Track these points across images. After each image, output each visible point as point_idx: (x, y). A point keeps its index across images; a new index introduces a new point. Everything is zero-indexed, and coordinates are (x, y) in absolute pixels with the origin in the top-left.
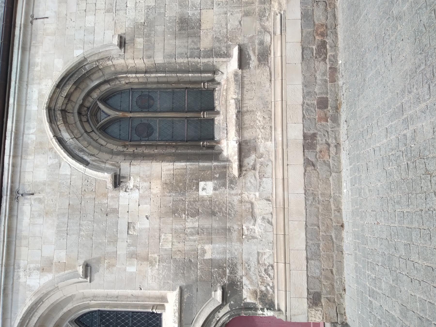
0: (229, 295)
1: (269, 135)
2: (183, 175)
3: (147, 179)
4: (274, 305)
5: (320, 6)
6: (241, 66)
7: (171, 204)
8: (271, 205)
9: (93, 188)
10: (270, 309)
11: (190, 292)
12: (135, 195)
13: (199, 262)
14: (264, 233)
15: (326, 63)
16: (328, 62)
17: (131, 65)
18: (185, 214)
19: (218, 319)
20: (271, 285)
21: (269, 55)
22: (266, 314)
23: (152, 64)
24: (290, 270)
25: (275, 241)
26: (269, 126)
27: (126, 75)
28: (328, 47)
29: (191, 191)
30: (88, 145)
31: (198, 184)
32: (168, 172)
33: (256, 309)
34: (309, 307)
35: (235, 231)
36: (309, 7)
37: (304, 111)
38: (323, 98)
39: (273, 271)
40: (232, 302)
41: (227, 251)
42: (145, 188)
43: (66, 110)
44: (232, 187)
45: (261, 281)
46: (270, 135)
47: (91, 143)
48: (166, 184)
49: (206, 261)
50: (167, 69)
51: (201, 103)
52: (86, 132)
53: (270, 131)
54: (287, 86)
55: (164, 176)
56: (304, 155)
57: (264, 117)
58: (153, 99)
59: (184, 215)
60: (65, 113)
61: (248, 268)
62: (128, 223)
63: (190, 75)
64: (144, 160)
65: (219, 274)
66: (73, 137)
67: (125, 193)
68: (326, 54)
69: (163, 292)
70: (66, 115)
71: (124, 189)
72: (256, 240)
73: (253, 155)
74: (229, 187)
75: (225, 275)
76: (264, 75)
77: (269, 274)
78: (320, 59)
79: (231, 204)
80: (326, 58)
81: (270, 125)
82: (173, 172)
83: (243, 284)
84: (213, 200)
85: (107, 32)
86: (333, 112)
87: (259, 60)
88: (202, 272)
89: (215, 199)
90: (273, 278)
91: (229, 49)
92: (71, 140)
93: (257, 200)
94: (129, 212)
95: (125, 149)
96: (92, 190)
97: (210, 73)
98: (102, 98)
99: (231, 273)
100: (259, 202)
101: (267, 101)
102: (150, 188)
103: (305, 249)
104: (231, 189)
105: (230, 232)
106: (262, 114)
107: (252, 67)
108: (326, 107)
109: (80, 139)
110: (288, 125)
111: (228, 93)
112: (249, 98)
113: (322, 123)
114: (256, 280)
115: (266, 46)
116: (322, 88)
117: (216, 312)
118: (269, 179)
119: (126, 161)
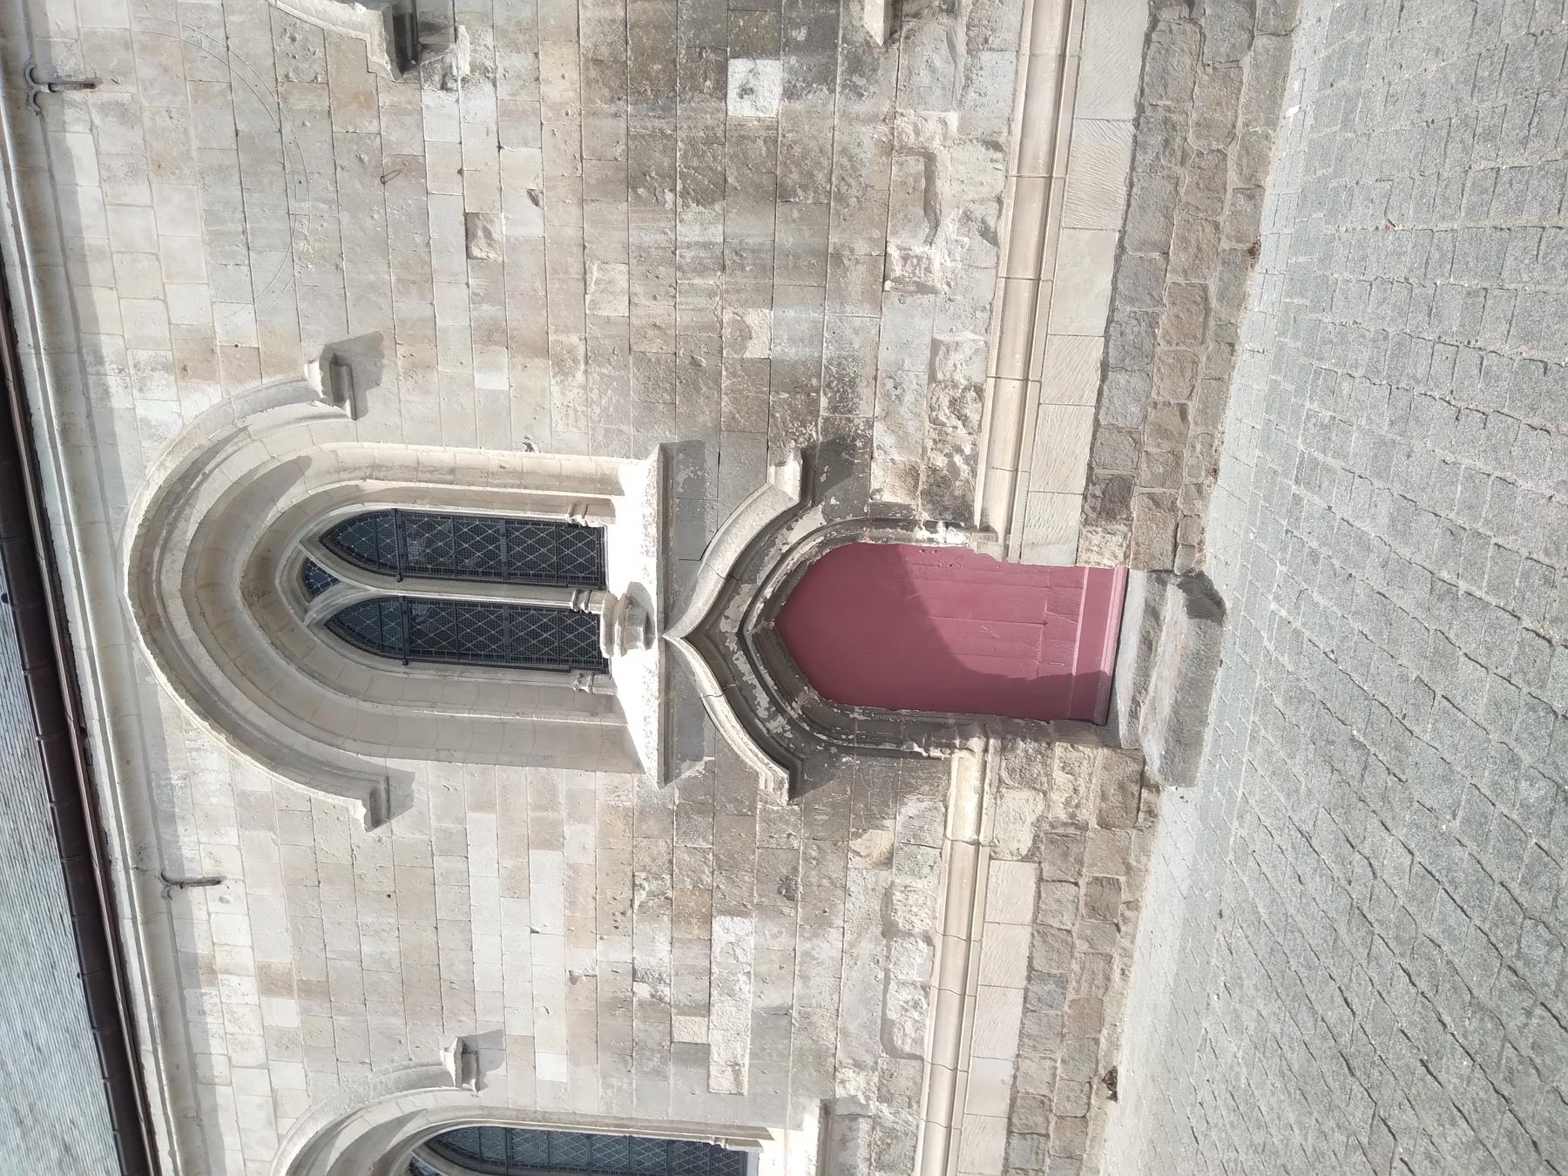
4: (971, 514)
7: (620, 149)
8: (999, 166)
10: (957, 526)
12: (482, 103)
20: (967, 450)
22: (941, 540)
31: (723, 69)
33: (910, 524)
35: (857, 262)
42: (518, 77)
45: (936, 437)
48: (598, 62)
61: (894, 392)
67: (442, 94)
71: (437, 78)
74: (844, 86)
77: (966, 416)
83: (875, 445)
84: (780, 139)
89: (790, 135)
93: (949, 143)
96: (316, 77)
102: (537, 79)
104: (851, 95)
105: (839, 267)
114: (919, 435)
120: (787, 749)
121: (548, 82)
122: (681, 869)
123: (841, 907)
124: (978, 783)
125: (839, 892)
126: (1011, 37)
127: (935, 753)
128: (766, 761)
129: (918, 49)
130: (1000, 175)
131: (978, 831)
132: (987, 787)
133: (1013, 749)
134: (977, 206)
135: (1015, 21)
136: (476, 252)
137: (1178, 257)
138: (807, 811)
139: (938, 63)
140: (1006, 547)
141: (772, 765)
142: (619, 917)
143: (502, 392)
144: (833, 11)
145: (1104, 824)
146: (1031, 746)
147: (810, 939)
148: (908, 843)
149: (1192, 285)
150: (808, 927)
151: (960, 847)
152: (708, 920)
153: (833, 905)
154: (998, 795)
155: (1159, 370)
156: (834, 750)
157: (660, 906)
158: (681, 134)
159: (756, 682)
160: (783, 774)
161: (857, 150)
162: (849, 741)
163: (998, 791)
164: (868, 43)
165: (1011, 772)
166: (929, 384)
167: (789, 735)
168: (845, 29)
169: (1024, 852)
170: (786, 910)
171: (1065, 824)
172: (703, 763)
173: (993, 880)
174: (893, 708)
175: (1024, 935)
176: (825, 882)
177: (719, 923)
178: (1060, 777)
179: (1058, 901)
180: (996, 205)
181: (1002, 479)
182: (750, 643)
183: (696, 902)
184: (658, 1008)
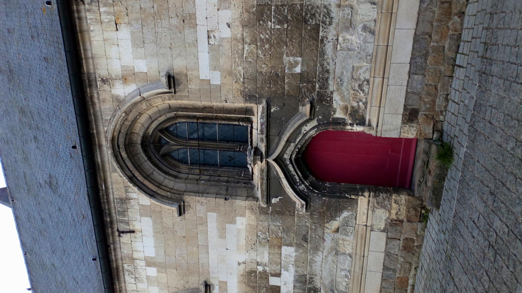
0: (317, 110)
4: (365, 121)
11: (276, 106)
13: (287, 76)
14: (363, 44)
18: (271, 21)
19: (305, 132)
20: (364, 100)
22: (355, 129)
24: (388, 85)
25: (374, 53)
33: (345, 124)
34: (403, 123)
35: (329, 42)
39: (368, 86)
40: (320, 117)
41: (318, 65)
45: (354, 96)
49: (293, 75)
59: (269, 23)
61: (340, 83)
62: (208, 31)
65: (308, 89)
69: (248, 105)
72: (353, 52)
75: (314, 90)
79: (327, 9)
84: (304, 4)
88: (289, 86)
89: (308, 3)
90: (367, 93)
93: (359, 3)
94: (208, 18)
99: (320, 88)
100: (361, 6)
103: (409, 62)
114: (348, 96)
117: (303, 126)
120: (305, 195)
122: (272, 231)
123: (322, 245)
124: (367, 207)
125: (322, 240)
127: (353, 197)
128: (298, 198)
130: (376, 13)
131: (367, 223)
132: (370, 208)
133: (379, 196)
134: (368, 23)
136: (211, 42)
137: (435, 37)
138: (311, 215)
140: (377, 132)
141: (300, 200)
142: (253, 245)
143: (218, 85)
145: (409, 221)
146: (385, 195)
147: (312, 254)
148: (344, 225)
149: (439, 46)
150: (312, 250)
151: (361, 227)
152: (280, 247)
153: (320, 244)
154: (373, 211)
155: (428, 74)
156: (320, 195)
157: (265, 242)
158: (273, 4)
159: (295, 174)
160: (304, 203)
161: (329, 7)
162: (325, 193)
163: (373, 209)
165: (378, 203)
166: (351, 80)
167: (306, 190)
169: (382, 229)
170: (305, 245)
171: (396, 220)
172: (278, 199)
173: (372, 237)
174: (339, 182)
175: (382, 255)
176: (317, 237)
177: (284, 248)
178: (394, 205)
179: (394, 245)
180: (374, 22)
181: (375, 110)
182: (293, 162)
183: (277, 241)
184: (265, 276)
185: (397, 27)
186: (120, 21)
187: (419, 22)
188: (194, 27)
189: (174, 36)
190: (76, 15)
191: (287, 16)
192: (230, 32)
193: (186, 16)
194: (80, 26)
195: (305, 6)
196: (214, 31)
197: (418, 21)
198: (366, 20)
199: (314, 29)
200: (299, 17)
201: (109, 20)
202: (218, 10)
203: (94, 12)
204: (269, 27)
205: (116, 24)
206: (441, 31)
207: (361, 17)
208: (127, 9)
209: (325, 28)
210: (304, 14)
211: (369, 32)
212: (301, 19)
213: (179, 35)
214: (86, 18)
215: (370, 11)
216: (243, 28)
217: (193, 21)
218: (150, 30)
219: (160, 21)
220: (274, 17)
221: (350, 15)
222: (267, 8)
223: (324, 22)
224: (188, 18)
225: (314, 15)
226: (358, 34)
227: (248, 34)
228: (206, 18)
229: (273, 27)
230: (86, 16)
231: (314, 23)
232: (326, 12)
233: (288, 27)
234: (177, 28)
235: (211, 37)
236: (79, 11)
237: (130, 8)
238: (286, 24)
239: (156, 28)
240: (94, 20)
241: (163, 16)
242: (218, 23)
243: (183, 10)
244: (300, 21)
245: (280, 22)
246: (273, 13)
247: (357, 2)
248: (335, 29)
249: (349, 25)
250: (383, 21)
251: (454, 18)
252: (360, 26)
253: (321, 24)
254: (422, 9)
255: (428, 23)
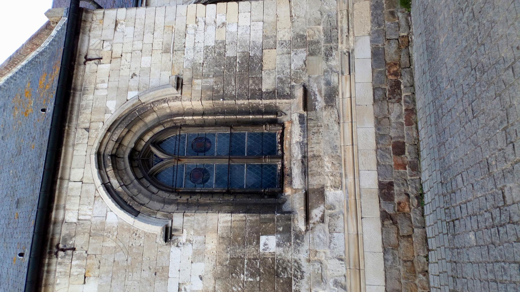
1: (339, 183)
2: (242, 229)
3: (201, 232)
5: (392, 44)
6: (305, 108)
7: (228, 262)
8: (343, 266)
9: (141, 242)
12: (188, 250)
15: (401, 105)
16: (403, 104)
17: (187, 107)
18: (243, 274)
21: (336, 96)
23: (210, 106)
26: (338, 173)
27: (182, 117)
28: (402, 87)
29: (251, 247)
30: (137, 193)
31: (258, 239)
32: (226, 225)
36: (380, 45)
37: (378, 157)
38: (399, 142)
42: (199, 243)
43: (117, 155)
44: (297, 243)
46: (340, 183)
47: (141, 190)
48: (223, 238)
50: (226, 111)
51: (262, 146)
52: (137, 178)
53: (340, 179)
54: (358, 130)
55: (221, 229)
56: (380, 206)
57: (332, 163)
58: (210, 142)
59: (242, 276)
60: (115, 159)
62: (179, 284)
63: (251, 117)
64: (198, 210)
66: (122, 184)
67: (177, 248)
68: (400, 95)
70: (116, 160)
71: (176, 244)
73: (321, 206)
74: (294, 243)
76: (331, 117)
78: (393, 100)
79: (298, 263)
80: (401, 99)
81: (340, 171)
82: (230, 225)
84: (276, 258)
85: (163, 73)
86: (412, 159)
87: (327, 102)
89: (279, 257)
91: (293, 90)
92: (120, 188)
94: (181, 271)
95: (178, 197)
97: (273, 115)
98: (155, 142)
100: (329, 261)
101: (336, 146)
102: (205, 243)
104: (296, 245)
106: (331, 160)
107: (318, 109)
108: (403, 152)
109: (129, 186)
110: (361, 172)
111: (293, 136)
112: (316, 141)
113: (400, 170)
115: (334, 87)
116: (398, 132)
118: (341, 234)
119: (179, 211)
121: (208, 243)
126: (342, 229)
129: (315, 232)
130: (344, 268)
134: (338, 278)
135: (342, 225)
139: (321, 236)
144: (290, 223)
161: (299, 261)
164: (300, 231)
168: (293, 227)
180: (344, 278)
185: (367, 283)
186: (90, 274)
187: (387, 279)
188: (165, 280)
189: (143, 289)
190: (46, 268)
191: (259, 269)
192: (202, 285)
193: (159, 269)
194: (47, 280)
195: (277, 260)
196: (185, 284)
197: (386, 278)
198: (336, 275)
199: (286, 282)
200: (271, 270)
201: (78, 273)
202: (192, 263)
203: (65, 265)
204: (242, 279)
205: (85, 277)
206: (411, 289)
207: (331, 272)
208: (100, 262)
209: (297, 282)
210: (276, 268)
211: (341, 287)
212: (273, 272)
213: (149, 288)
214: (55, 271)
215: (339, 267)
216: (215, 281)
217: (165, 274)
218: (119, 283)
219: (131, 274)
220: (247, 270)
221: (320, 270)
222: (239, 261)
223: (295, 276)
224: (160, 270)
225: (285, 268)
226: (330, 289)
227: (220, 286)
228: (179, 271)
229: (245, 280)
230: (56, 269)
231: (286, 277)
232: (297, 266)
233: (260, 280)
234: (148, 280)
235: (181, 290)
236: (49, 265)
237: (103, 261)
238: (259, 277)
239: (126, 281)
240: (63, 273)
241: (135, 269)
242: (191, 276)
243: (157, 263)
244: (272, 274)
245: (252, 275)
246: (245, 266)
247: (326, 258)
248: (307, 283)
249: (320, 280)
250: (352, 276)
251: (419, 276)
252: (332, 280)
253: (293, 277)
254: (387, 267)
255: (396, 281)
